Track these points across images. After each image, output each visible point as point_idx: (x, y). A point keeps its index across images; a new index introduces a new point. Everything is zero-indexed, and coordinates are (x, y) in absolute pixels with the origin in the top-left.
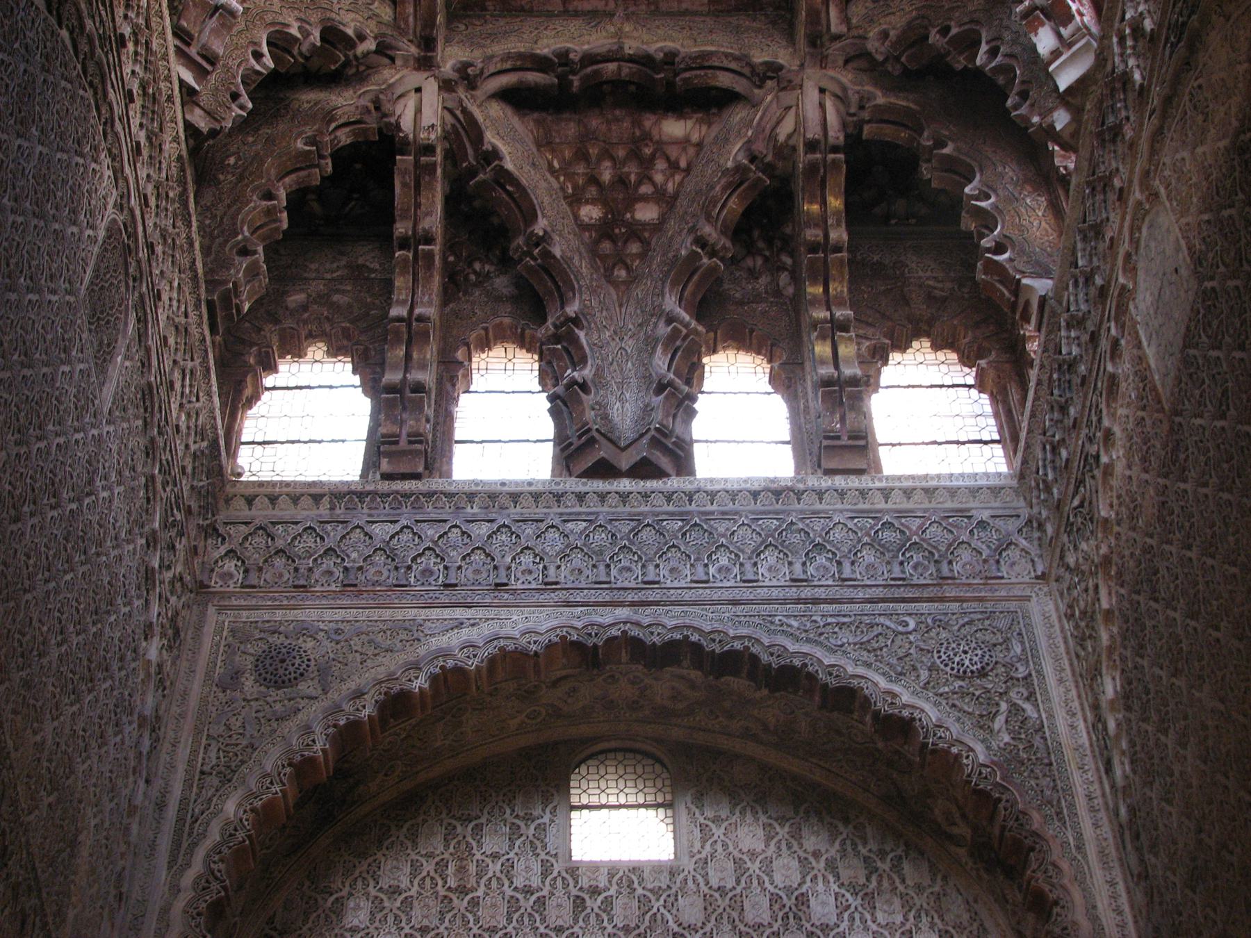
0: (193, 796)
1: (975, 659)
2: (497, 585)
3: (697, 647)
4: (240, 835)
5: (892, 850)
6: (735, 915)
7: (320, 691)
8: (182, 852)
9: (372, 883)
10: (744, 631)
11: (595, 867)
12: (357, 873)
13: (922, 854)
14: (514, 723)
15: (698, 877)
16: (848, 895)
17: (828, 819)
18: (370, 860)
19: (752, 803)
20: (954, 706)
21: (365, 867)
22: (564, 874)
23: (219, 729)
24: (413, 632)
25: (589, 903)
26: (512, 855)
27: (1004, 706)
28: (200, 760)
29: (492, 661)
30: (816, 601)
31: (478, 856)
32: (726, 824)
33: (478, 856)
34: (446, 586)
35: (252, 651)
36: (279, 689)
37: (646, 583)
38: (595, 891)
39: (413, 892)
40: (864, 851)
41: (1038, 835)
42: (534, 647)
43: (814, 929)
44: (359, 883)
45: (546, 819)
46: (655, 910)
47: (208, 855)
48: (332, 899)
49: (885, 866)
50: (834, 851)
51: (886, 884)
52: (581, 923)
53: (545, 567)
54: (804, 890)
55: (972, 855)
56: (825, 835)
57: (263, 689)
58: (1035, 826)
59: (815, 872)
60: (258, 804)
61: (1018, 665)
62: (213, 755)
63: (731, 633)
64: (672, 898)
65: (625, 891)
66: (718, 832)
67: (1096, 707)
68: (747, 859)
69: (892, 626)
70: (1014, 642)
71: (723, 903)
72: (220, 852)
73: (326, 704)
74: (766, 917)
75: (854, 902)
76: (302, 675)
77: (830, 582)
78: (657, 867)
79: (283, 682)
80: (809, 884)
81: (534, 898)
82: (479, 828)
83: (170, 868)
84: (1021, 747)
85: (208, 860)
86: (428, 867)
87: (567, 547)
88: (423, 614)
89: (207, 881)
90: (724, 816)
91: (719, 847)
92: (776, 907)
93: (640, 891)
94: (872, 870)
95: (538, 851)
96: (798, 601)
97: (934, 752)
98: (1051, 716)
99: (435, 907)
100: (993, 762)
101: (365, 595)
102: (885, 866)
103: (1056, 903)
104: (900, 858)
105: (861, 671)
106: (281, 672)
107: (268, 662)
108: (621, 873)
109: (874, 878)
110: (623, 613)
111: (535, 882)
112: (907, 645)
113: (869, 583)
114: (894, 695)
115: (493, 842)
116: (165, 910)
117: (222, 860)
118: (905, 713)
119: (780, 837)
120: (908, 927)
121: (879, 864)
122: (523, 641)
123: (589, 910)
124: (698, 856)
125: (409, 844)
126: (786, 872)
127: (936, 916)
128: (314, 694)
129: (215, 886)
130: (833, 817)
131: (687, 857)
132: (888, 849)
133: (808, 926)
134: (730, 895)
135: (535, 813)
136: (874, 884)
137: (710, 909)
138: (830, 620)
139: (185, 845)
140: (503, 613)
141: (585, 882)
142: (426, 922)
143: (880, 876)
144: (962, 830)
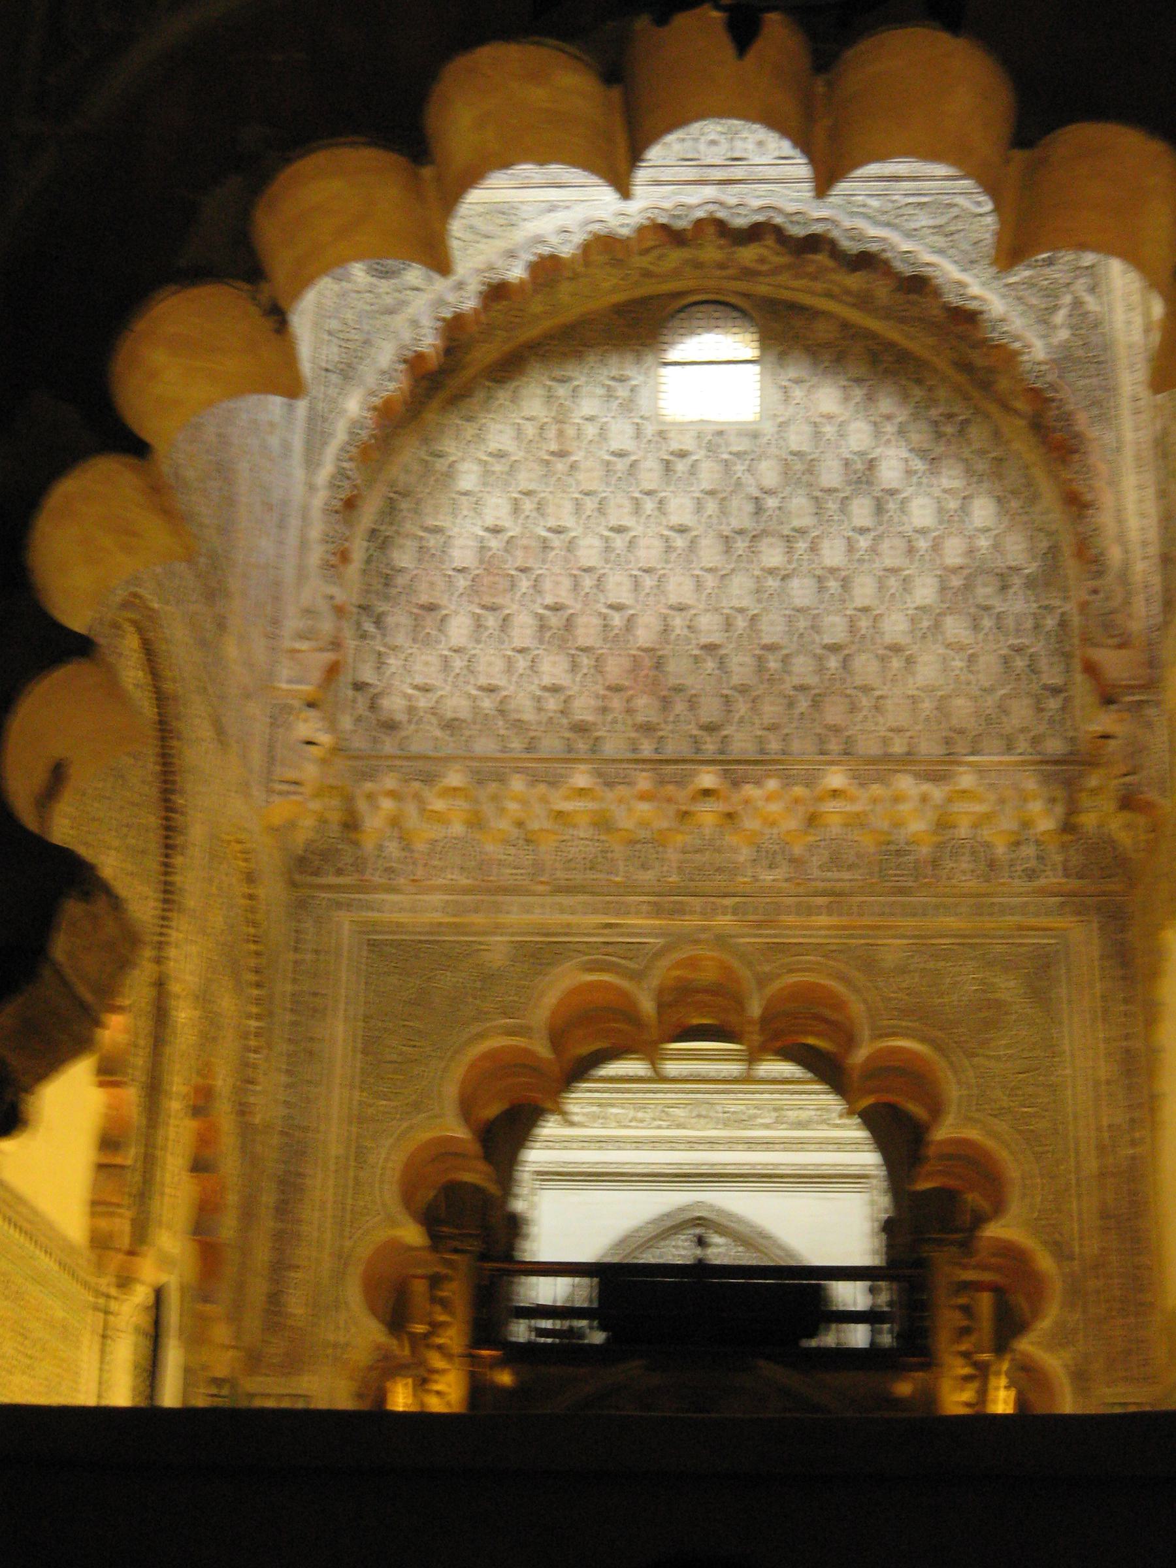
3: (778, 230)
10: (824, 213)
11: (682, 427)
14: (606, 285)
23: (334, 324)
24: (507, 215)
29: (586, 247)
38: (682, 454)
42: (625, 232)
49: (949, 430)
60: (377, 401)
66: (798, 393)
71: (799, 466)
73: (432, 296)
75: (919, 465)
78: (740, 434)
82: (575, 389)
86: (530, 430)
94: (939, 435)
99: (540, 470)
110: (710, 192)
115: (588, 405)
117: (351, 459)
118: (973, 305)
126: (859, 435)
129: (346, 483)
141: (675, 446)
142: (532, 486)
144: (1019, 405)
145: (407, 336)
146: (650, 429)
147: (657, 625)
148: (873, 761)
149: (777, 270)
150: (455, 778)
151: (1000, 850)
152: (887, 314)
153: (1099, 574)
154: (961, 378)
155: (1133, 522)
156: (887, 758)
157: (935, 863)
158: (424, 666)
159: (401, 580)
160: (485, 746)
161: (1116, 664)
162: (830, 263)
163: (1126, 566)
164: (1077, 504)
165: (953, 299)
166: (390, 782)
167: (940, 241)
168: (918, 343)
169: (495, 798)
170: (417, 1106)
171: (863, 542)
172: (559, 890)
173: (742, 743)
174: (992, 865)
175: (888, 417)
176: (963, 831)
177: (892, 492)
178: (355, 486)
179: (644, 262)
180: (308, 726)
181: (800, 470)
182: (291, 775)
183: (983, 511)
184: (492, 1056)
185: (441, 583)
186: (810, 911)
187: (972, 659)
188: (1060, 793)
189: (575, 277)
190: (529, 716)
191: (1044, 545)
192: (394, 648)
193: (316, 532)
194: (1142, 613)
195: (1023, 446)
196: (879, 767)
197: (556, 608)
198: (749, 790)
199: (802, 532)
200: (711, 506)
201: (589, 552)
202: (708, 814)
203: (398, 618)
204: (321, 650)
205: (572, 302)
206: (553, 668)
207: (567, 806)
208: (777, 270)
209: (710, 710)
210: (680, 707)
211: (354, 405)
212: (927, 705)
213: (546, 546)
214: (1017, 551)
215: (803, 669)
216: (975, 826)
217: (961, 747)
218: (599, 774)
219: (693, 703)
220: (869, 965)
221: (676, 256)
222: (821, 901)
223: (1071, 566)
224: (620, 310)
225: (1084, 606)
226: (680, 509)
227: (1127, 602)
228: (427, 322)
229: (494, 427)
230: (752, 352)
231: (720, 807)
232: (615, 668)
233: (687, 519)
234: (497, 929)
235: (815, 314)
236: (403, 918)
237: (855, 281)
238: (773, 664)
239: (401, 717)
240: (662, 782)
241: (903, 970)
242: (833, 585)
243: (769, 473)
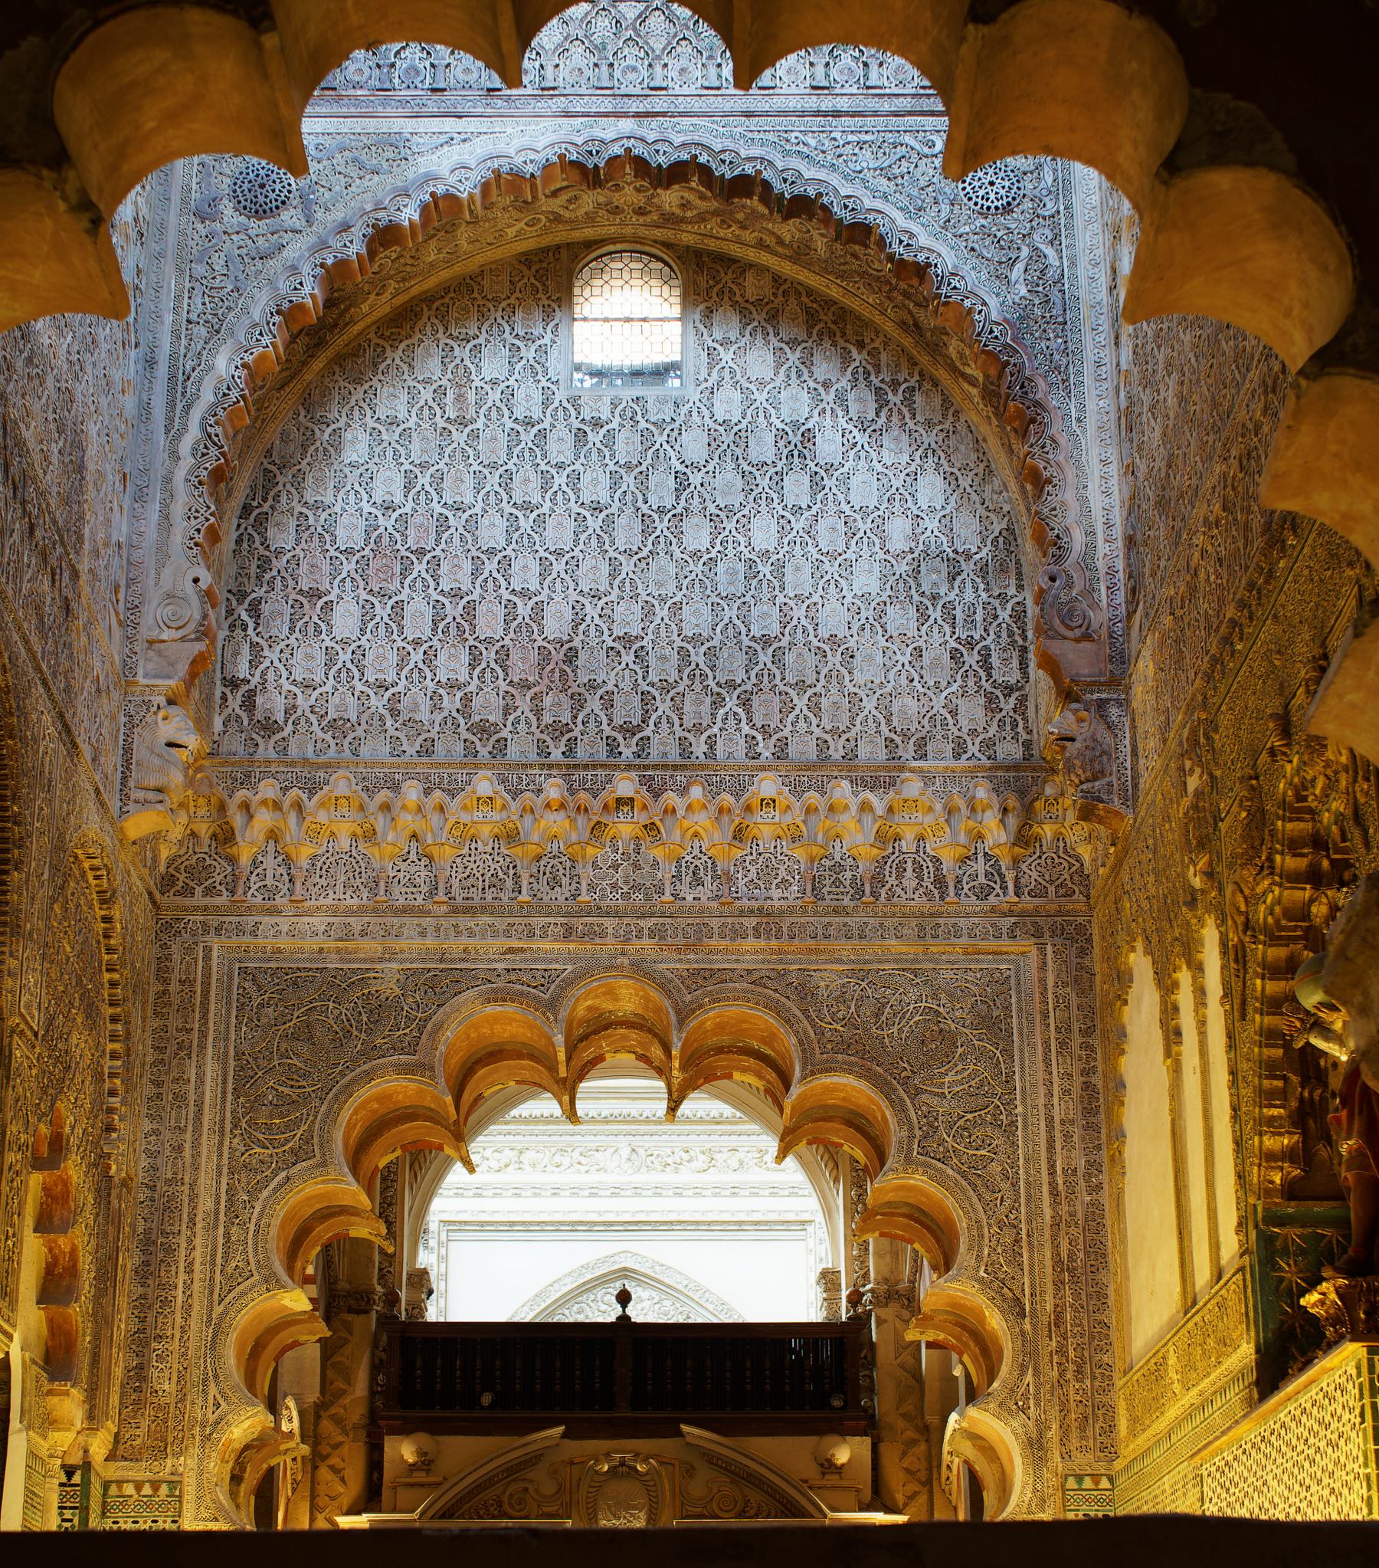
0: (183, 351)
1: (1002, 192)
2: (489, 90)
3: (705, 171)
4: (234, 394)
5: (906, 380)
6: (739, 452)
7: (304, 223)
8: (178, 415)
9: (369, 413)
12: (353, 403)
13: (936, 385)
14: (511, 232)
15: (704, 409)
16: (855, 432)
17: (841, 342)
18: (366, 386)
19: (763, 324)
20: (973, 249)
21: (361, 395)
22: (565, 404)
23: (200, 269)
25: (591, 436)
26: (512, 382)
27: (1025, 252)
28: (186, 307)
29: (486, 187)
30: (837, 114)
31: (477, 383)
32: (734, 347)
33: (477, 383)
34: (434, 90)
35: (227, 171)
36: (260, 220)
37: (652, 89)
38: (597, 424)
39: (411, 424)
40: (876, 381)
41: (1041, 405)
42: (530, 168)
43: (817, 469)
44: (356, 412)
45: (547, 340)
46: (657, 446)
47: (204, 418)
48: (329, 430)
49: (895, 399)
50: (844, 383)
51: (895, 419)
52: (582, 460)
53: (542, 66)
54: (810, 425)
55: (983, 398)
56: (837, 362)
57: (242, 219)
58: (1039, 396)
59: (824, 404)
60: (249, 359)
61: (1046, 200)
62: (199, 301)
63: (743, 153)
64: (676, 432)
65: (628, 424)
66: (726, 356)
67: (1114, 271)
68: (754, 389)
69: (917, 147)
70: (1046, 169)
71: (728, 439)
72: (216, 415)
74: (769, 457)
75: (861, 438)
76: (283, 203)
77: (854, 90)
79: (265, 212)
80: (816, 418)
81: (534, 430)
83: (167, 432)
84: (1037, 302)
85: (204, 425)
86: (427, 395)
87: (566, 39)
88: (408, 126)
89: (206, 447)
90: (733, 339)
91: (726, 373)
92: (781, 444)
93: (643, 424)
94: (882, 404)
95: (539, 377)
96: (818, 113)
97: (946, 304)
98: (1073, 264)
100: (1005, 320)
101: (346, 100)
102: (895, 399)
103: (1049, 481)
104: (913, 389)
105: (878, 204)
106: (261, 199)
107: (246, 186)
108: (624, 404)
109: (883, 414)
110: (627, 126)
111: (536, 414)
112: (931, 172)
113: (896, 91)
114: (912, 235)
115: (492, 365)
116: (168, 480)
117: (217, 423)
118: (921, 258)
119: (789, 363)
120: (913, 468)
121: (890, 396)
122: (518, 160)
123: (590, 445)
124: (704, 385)
125: (405, 368)
126: (796, 403)
127: (943, 456)
128: (298, 226)
129: (214, 451)
130: (847, 341)
131: (693, 386)
132: (902, 380)
133: (812, 465)
134: (736, 429)
135: (536, 333)
136: (882, 420)
137: (714, 445)
138: (851, 138)
139: (179, 406)
140: (498, 124)
141: (586, 413)
143: (890, 410)
145: (284, 286)
146: (560, 395)
147: (569, 615)
148: (809, 766)
149: (702, 218)
150: (341, 784)
151: (947, 866)
152: (825, 268)
153: (1058, 559)
154: (907, 342)
155: (1097, 501)
156: (823, 761)
157: (878, 879)
158: (308, 661)
159: (279, 564)
160: (375, 749)
161: (1079, 659)
162: (762, 209)
163: (1091, 547)
164: (1036, 482)
165: (897, 248)
166: (268, 789)
167: (884, 184)
168: (863, 302)
169: (386, 807)
170: (297, 1156)
171: (799, 524)
172: (455, 911)
173: (663, 746)
174: (940, 882)
175: (826, 385)
176: (907, 845)
177: (829, 468)
178: (223, 454)
179: (556, 205)
180: (175, 725)
181: (728, 442)
183: (931, 490)
184: (381, 1098)
185: (326, 568)
186: (738, 934)
187: (919, 652)
188: (1012, 802)
189: (475, 222)
190: (424, 715)
191: (998, 526)
192: (272, 641)
194: (1106, 605)
195: (976, 414)
196: (813, 773)
197: (456, 594)
198: (671, 798)
199: (730, 511)
200: (629, 480)
201: (492, 531)
202: (625, 827)
203: (276, 606)
205: (471, 248)
206: (452, 663)
207: (465, 818)
208: (702, 218)
209: (628, 710)
210: (594, 704)
211: (224, 364)
212: (869, 704)
213: (443, 524)
214: (968, 532)
215: (734, 666)
216: (921, 838)
217: (907, 752)
218: (504, 781)
219: (608, 702)
220: (805, 993)
221: (590, 199)
222: (750, 922)
223: (1028, 548)
224: (526, 259)
225: (1040, 596)
226: (595, 486)
227: (1090, 591)
228: (306, 269)
229: (385, 392)
230: (676, 311)
231: (642, 818)
232: (522, 665)
233: (604, 497)
234: (390, 955)
235: (744, 268)
236: (284, 943)
237: (789, 230)
238: (698, 657)
239: (280, 717)
240: (572, 792)
241: (842, 999)
242: (765, 569)
243: (694, 446)
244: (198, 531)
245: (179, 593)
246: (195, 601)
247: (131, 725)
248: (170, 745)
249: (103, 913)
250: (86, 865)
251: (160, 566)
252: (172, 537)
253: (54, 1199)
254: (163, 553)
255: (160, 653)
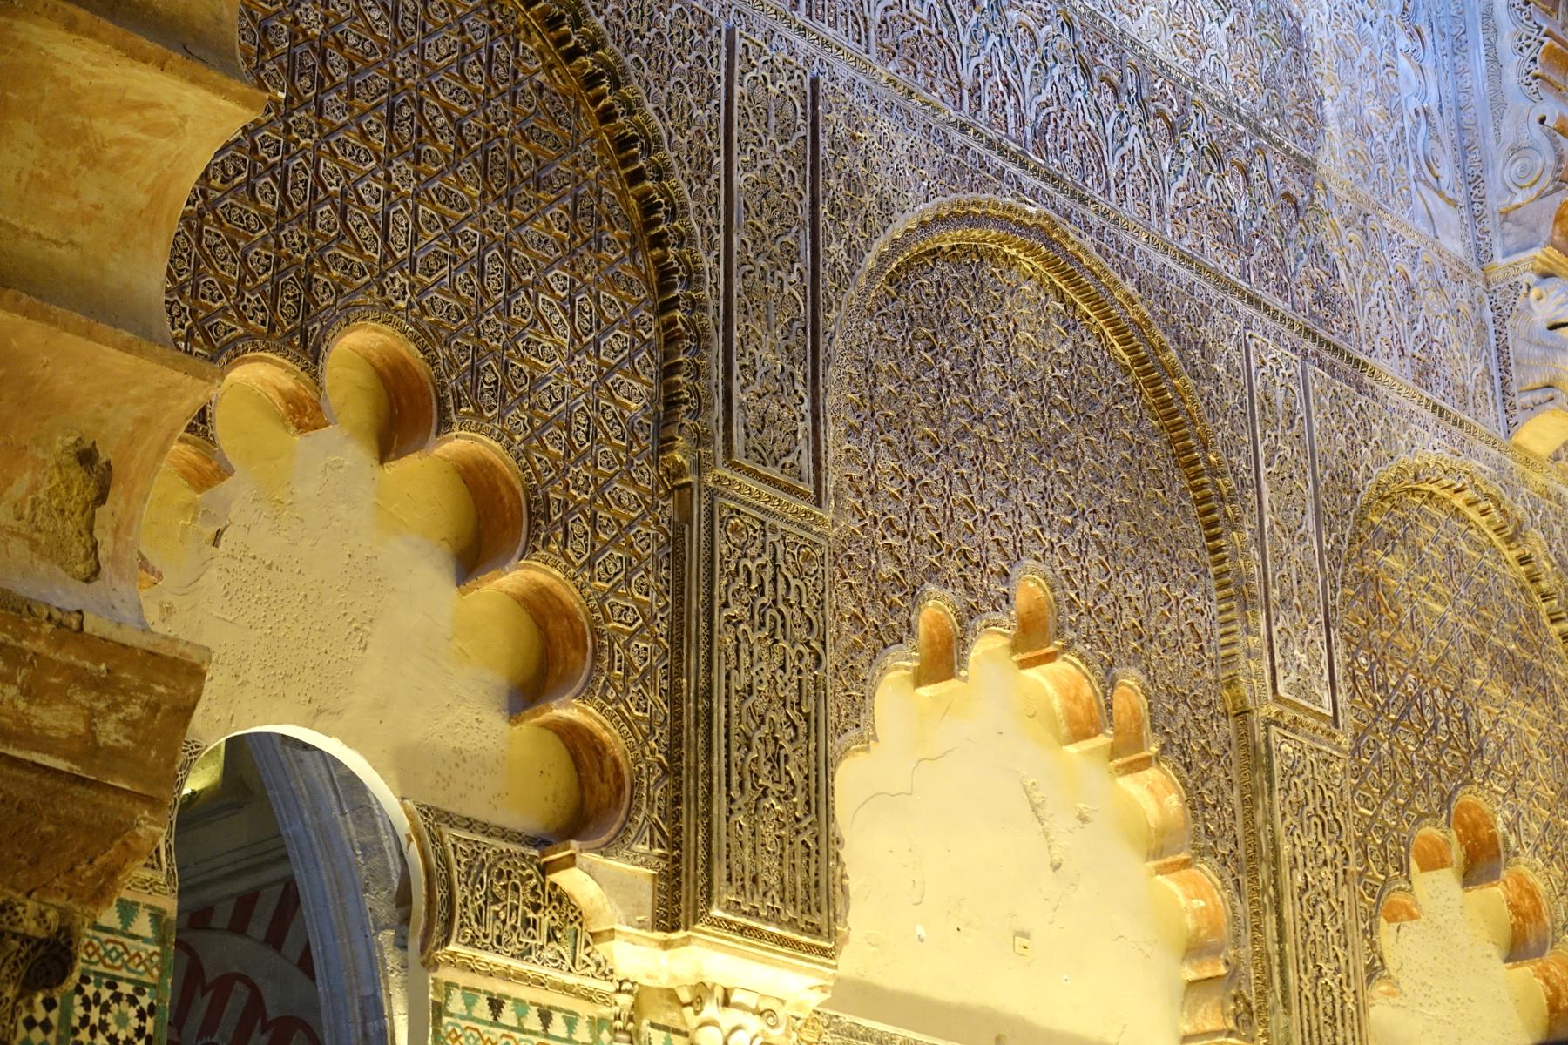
182: (1539, 379)
193: (1506, 43)
204: (1541, 196)
244: (1534, 60)
245: (1525, 143)
246: (1546, 145)
247: (1500, 319)
248: (1554, 327)
249: (1515, 553)
250: (1458, 501)
251: (1498, 119)
252: (1504, 80)
253: (1525, 916)
254: (1498, 103)
255: (1518, 223)
